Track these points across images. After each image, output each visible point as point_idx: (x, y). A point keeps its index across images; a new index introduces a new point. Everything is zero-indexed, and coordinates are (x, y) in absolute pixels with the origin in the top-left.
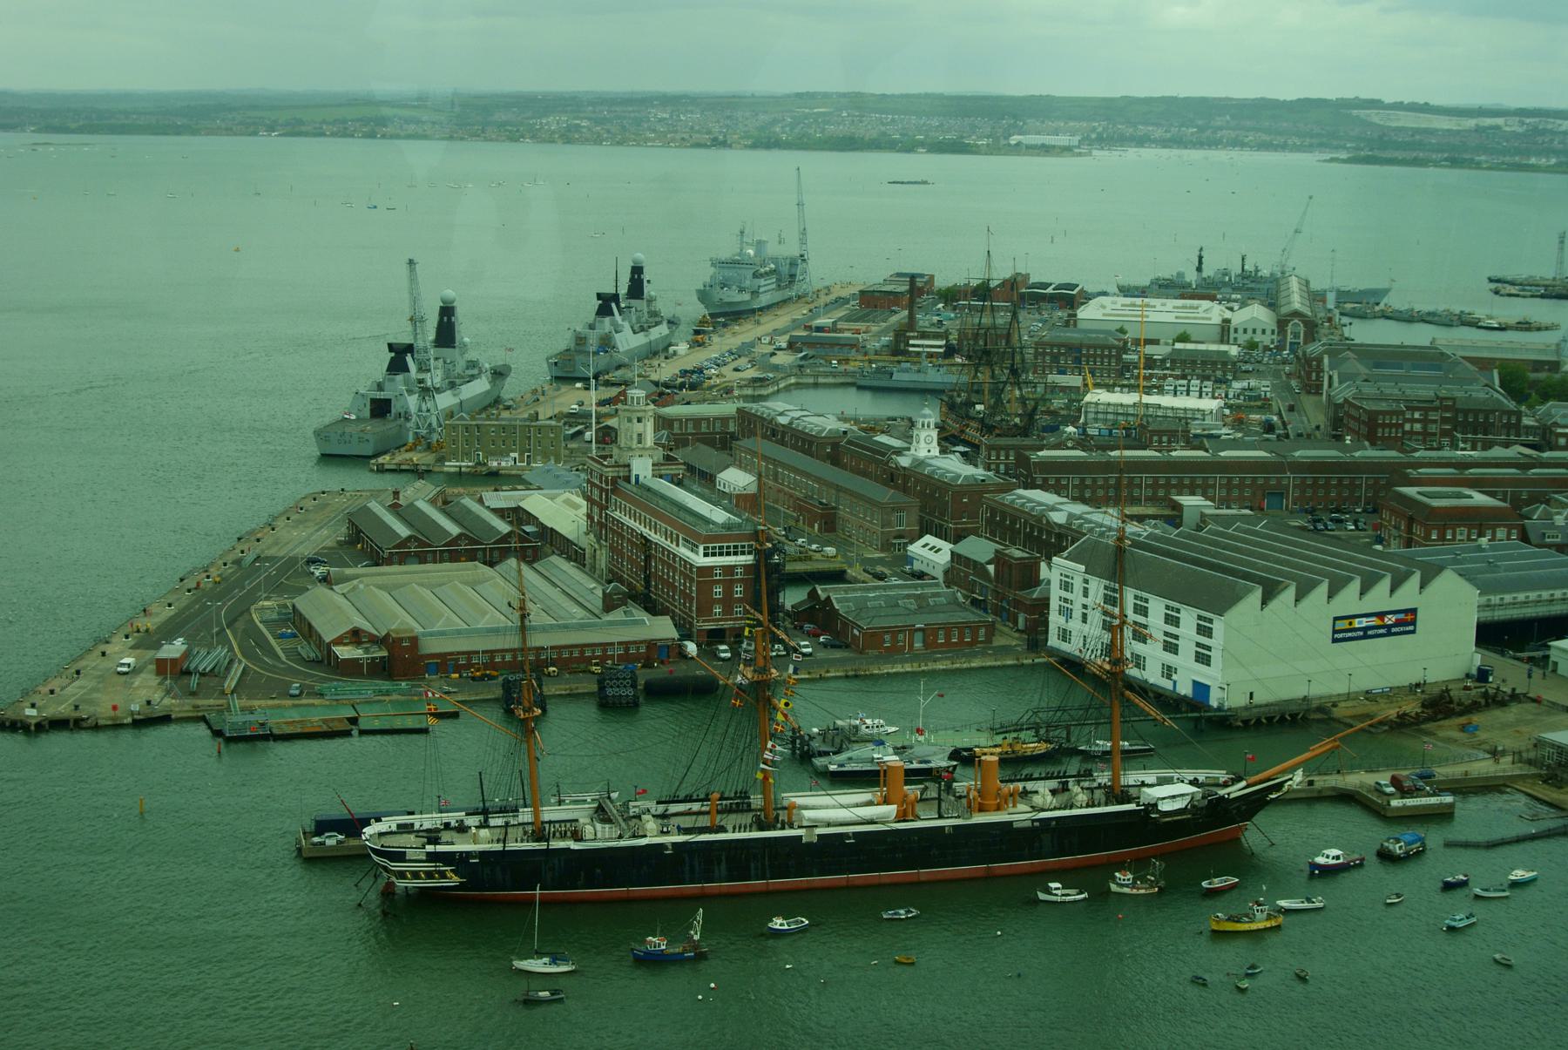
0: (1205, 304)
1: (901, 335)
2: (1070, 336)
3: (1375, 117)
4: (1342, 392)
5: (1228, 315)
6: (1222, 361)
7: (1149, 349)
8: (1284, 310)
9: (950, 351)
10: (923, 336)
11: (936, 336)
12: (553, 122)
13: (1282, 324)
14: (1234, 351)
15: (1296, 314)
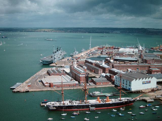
0: (132, 49)
1: (102, 51)
2: (118, 53)
3: (148, 30)
4: (145, 58)
5: (134, 50)
6: (133, 55)
7: (126, 54)
8: (139, 50)
9: (107, 54)
10: (104, 52)
11: (105, 52)
12: (69, 30)
13: (139, 51)
14: (134, 54)
15: (140, 50)
